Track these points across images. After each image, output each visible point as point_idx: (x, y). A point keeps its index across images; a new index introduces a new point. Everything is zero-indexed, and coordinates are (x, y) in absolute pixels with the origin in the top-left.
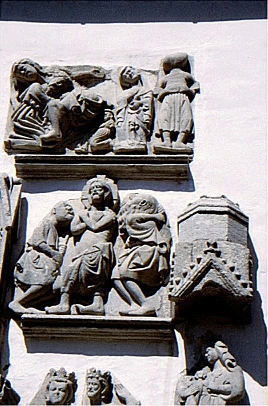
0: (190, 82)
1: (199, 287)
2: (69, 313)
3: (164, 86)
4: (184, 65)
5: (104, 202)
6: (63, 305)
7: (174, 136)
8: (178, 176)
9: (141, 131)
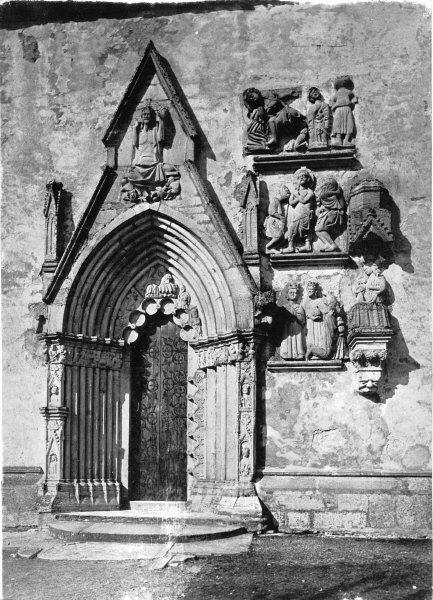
0: (351, 96)
1: (365, 237)
2: (294, 252)
3: (335, 101)
4: (348, 84)
5: (309, 183)
6: (290, 248)
7: (343, 136)
8: (350, 162)
9: (323, 135)
